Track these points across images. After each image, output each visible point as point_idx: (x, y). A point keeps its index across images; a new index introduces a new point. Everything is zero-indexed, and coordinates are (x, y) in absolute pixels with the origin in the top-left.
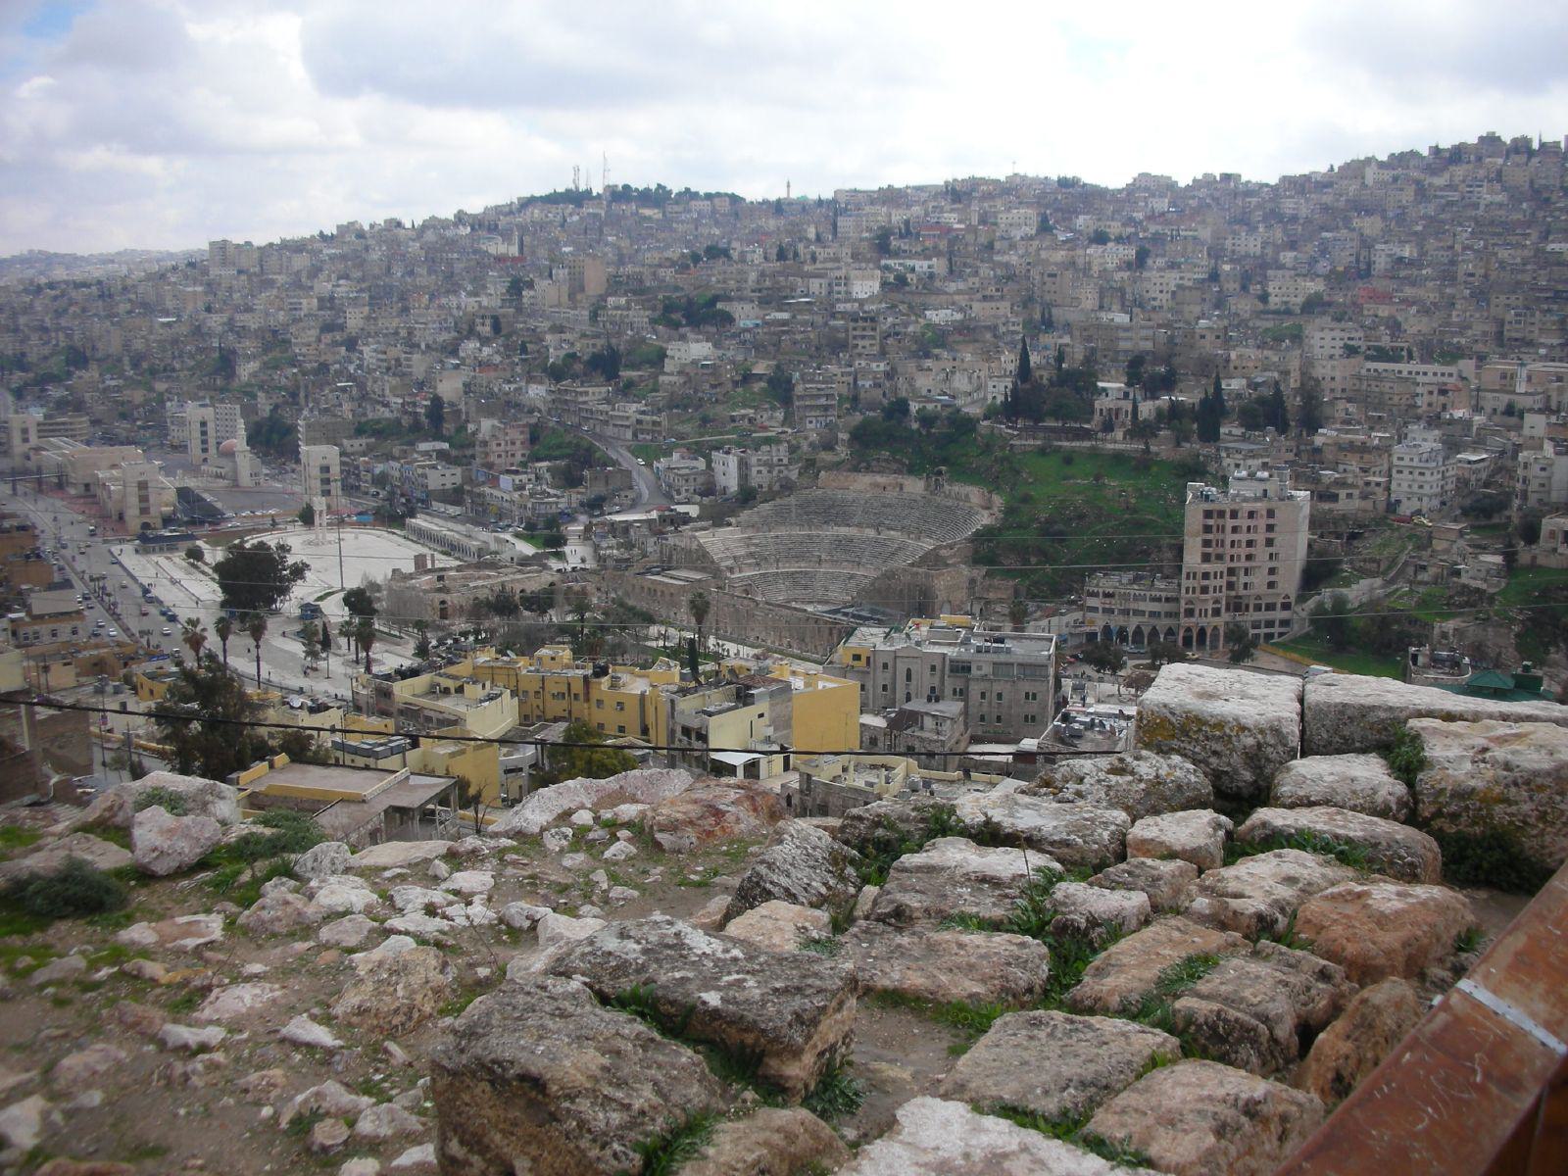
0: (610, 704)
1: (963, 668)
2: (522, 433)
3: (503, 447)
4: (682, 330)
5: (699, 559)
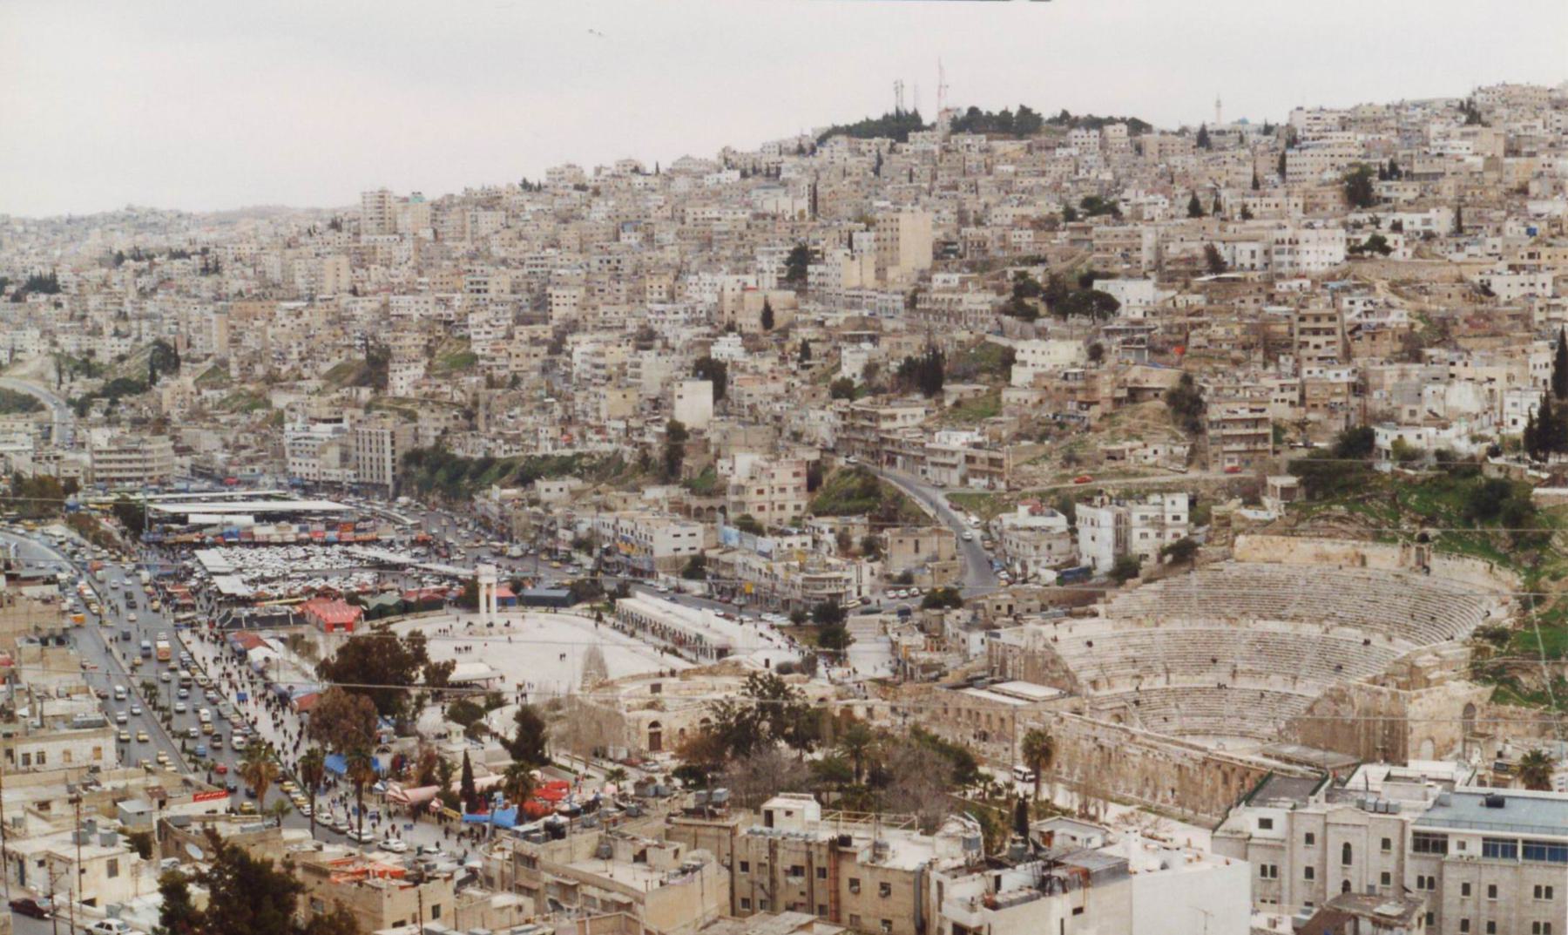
0: (869, 883)
1: (1435, 844)
2: (796, 475)
3: (766, 496)
4: (1039, 323)
5: (1045, 668)
